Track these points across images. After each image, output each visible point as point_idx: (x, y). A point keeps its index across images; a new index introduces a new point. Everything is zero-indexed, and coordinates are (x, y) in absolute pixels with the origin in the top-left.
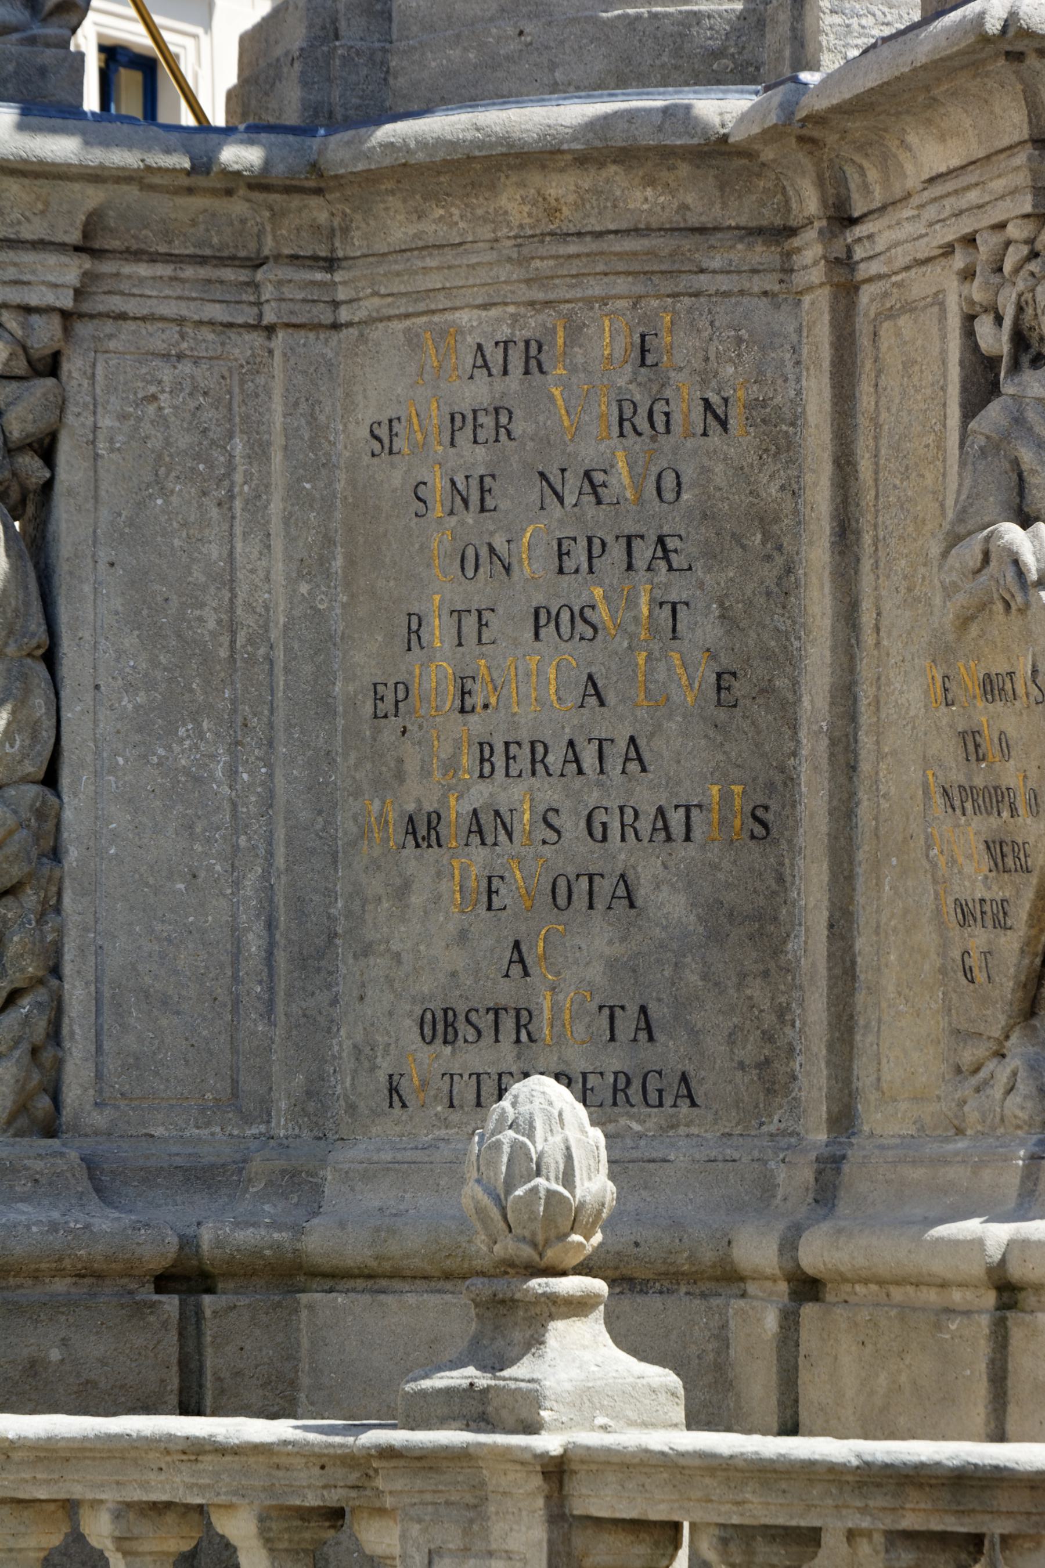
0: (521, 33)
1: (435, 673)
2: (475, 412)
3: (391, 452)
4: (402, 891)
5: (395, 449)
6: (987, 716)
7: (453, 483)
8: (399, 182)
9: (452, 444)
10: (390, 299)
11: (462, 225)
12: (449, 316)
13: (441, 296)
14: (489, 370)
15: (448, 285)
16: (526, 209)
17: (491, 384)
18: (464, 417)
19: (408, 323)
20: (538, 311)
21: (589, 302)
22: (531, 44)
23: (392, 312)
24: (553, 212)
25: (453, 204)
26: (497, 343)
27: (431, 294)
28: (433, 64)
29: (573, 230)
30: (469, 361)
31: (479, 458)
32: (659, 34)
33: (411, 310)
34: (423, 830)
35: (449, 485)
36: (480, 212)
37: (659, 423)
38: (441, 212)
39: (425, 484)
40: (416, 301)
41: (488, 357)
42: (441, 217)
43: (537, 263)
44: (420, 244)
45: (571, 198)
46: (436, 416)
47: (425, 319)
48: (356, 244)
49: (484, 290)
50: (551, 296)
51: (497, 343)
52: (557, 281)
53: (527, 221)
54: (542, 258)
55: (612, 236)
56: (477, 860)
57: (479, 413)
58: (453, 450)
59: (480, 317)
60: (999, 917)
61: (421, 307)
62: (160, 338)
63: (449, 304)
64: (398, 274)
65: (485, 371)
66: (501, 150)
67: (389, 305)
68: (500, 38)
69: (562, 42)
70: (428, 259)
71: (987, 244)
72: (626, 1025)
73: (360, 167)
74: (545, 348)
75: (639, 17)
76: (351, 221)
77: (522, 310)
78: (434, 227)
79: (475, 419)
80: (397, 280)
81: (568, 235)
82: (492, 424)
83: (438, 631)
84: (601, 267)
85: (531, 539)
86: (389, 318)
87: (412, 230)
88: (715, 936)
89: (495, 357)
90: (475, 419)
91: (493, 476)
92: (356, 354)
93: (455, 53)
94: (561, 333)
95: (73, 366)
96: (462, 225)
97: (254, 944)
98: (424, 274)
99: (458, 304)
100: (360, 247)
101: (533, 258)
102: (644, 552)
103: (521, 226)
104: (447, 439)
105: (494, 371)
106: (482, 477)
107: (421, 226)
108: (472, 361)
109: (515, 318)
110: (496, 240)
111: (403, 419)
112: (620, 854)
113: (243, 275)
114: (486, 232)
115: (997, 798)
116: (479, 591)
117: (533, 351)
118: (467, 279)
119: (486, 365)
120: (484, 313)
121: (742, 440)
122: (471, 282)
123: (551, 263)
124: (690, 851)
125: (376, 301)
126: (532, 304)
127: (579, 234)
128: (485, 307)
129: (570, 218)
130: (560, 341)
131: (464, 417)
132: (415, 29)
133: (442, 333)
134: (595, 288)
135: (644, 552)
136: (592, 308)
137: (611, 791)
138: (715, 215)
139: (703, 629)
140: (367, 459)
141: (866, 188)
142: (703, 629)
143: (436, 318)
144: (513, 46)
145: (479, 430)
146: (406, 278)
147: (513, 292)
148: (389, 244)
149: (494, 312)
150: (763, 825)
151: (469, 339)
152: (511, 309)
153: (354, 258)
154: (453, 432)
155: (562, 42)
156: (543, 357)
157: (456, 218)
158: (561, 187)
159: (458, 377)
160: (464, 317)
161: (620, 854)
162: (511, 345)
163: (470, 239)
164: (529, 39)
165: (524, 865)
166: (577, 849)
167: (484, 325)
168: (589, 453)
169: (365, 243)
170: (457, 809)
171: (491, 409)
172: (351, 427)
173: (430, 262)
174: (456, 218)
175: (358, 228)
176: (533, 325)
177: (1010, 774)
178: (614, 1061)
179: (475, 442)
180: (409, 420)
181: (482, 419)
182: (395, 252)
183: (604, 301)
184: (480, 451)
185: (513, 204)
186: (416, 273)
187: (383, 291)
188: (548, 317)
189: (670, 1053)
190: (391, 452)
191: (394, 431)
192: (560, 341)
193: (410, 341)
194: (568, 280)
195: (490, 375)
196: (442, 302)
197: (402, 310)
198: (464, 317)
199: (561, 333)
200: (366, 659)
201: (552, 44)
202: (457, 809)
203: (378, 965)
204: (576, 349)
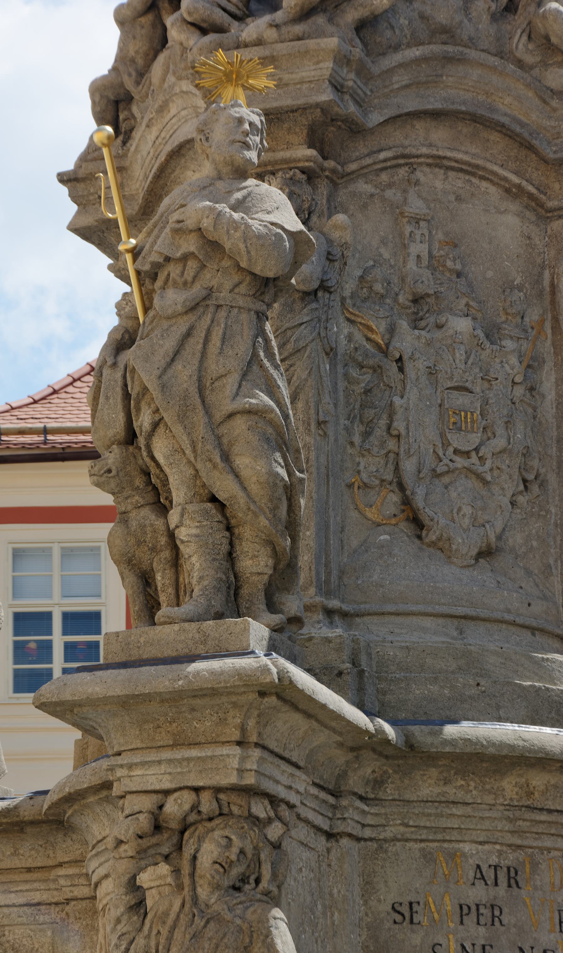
0: (478, 685)
2: (477, 906)
3: (412, 922)
5: (415, 921)
7: (463, 947)
8: (452, 761)
9: (462, 923)
10: (413, 829)
11: (474, 792)
12: (456, 845)
13: (455, 833)
14: (485, 881)
15: (463, 827)
16: (516, 789)
17: (487, 890)
18: (469, 908)
19: (423, 845)
20: (514, 851)
21: (541, 849)
22: (484, 692)
23: (414, 837)
24: (530, 794)
25: (472, 779)
26: (490, 866)
27: (447, 831)
28: (418, 692)
29: (539, 806)
30: (471, 874)
31: (481, 934)
32: (550, 700)
33: (431, 838)
35: (459, 948)
36: (488, 787)
38: (463, 782)
39: (441, 945)
40: (435, 833)
41: (484, 873)
42: (462, 786)
43: (520, 823)
44: (443, 799)
45: (542, 788)
46: (449, 905)
47: (436, 844)
48: (389, 791)
49: (484, 833)
50: (525, 843)
51: (490, 866)
52: (528, 835)
53: (515, 797)
54: (524, 820)
55: (556, 813)
57: (481, 907)
58: (461, 927)
59: (477, 849)
61: (439, 837)
63: (460, 838)
64: (429, 815)
65: (482, 881)
66: (540, 755)
67: (412, 832)
68: (465, 684)
69: (503, 694)
70: (454, 810)
73: (447, 749)
74: (519, 873)
75: (540, 688)
76: (389, 777)
77: (504, 848)
78: (454, 790)
79: (478, 910)
80: (425, 819)
81: (536, 809)
82: (490, 914)
84: (553, 831)
86: (407, 840)
87: (437, 790)
89: (490, 875)
90: (478, 910)
91: (491, 946)
92: (377, 859)
93: (434, 688)
94: (528, 866)
96: (474, 792)
98: (448, 818)
99: (466, 839)
100: (391, 794)
101: (520, 819)
103: (511, 799)
104: (458, 920)
105: (489, 882)
106: (484, 947)
107: (446, 789)
108: (473, 875)
109: (500, 853)
110: (494, 805)
111: (421, 903)
113: (331, 800)
114: (489, 799)
117: (512, 874)
118: (476, 825)
119: (483, 878)
120: (480, 847)
122: (479, 827)
123: (528, 824)
125: (402, 829)
126: (510, 846)
127: (541, 810)
128: (481, 843)
129: (537, 800)
130: (528, 870)
131: (469, 908)
132: (393, 668)
133: (452, 856)
136: (543, 854)
140: (388, 924)
143: (446, 845)
144: (474, 691)
145: (481, 917)
146: (432, 818)
147: (503, 837)
148: (418, 796)
149: (486, 847)
151: (471, 861)
152: (498, 847)
153: (382, 800)
154: (462, 916)
155: (503, 694)
156: (518, 878)
157: (471, 788)
158: (539, 780)
159: (464, 883)
160: (467, 847)
162: (498, 868)
163: (479, 801)
164: (483, 689)
167: (480, 854)
169: (397, 792)
171: (488, 905)
172: (373, 903)
173: (454, 811)
174: (471, 788)
175: (392, 783)
176: (511, 858)
179: (478, 923)
180: (426, 904)
181: (482, 910)
182: (420, 801)
183: (549, 850)
184: (482, 930)
185: (509, 786)
186: (442, 816)
187: (411, 823)
188: (520, 855)
190: (412, 922)
191: (414, 910)
192: (528, 870)
193: (425, 857)
194: (534, 835)
195: (486, 884)
196: (455, 836)
197: (423, 837)
198: (467, 847)
199: (528, 866)
201: (497, 694)
204: (537, 877)
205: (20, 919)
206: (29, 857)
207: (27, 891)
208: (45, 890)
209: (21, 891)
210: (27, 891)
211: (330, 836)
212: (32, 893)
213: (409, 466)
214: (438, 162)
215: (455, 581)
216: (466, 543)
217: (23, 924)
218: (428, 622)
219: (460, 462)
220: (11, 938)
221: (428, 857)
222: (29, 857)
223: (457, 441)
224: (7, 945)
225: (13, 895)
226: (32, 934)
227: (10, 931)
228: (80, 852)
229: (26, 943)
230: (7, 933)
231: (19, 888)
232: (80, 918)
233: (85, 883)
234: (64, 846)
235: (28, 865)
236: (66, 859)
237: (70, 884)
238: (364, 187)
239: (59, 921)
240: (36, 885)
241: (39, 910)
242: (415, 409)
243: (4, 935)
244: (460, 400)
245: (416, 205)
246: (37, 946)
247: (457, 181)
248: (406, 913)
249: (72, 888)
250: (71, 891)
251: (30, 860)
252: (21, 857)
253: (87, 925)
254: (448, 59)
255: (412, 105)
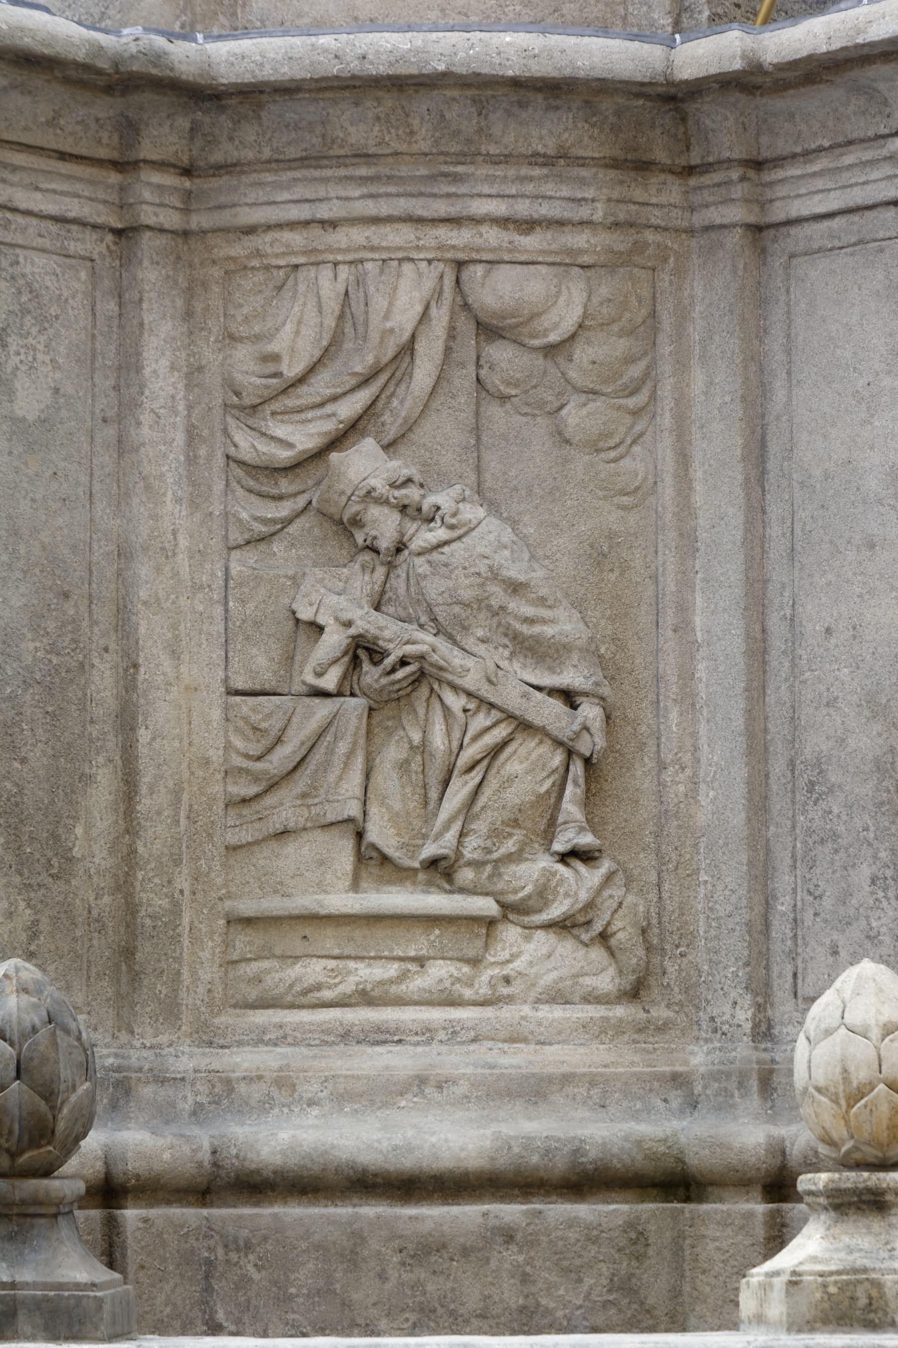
205: (40, 240)
206: (71, 134)
207: (62, 193)
208: (91, 199)
209: (54, 192)
210: (62, 193)
212: (68, 200)
217: (43, 250)
220: (27, 270)
222: (71, 134)
224: (21, 282)
225: (39, 196)
226: (58, 270)
227: (25, 258)
228: (174, 148)
229: (49, 284)
230: (21, 260)
231: (53, 186)
232: (158, 263)
233: (179, 205)
234: (156, 133)
235: (61, 148)
236: (154, 157)
237: (157, 201)
239: (96, 257)
240: (79, 187)
241: (69, 231)
243: (18, 263)
246: (66, 293)
249: (157, 210)
250: (156, 214)
251: (70, 140)
252: (59, 131)
253: (168, 277)
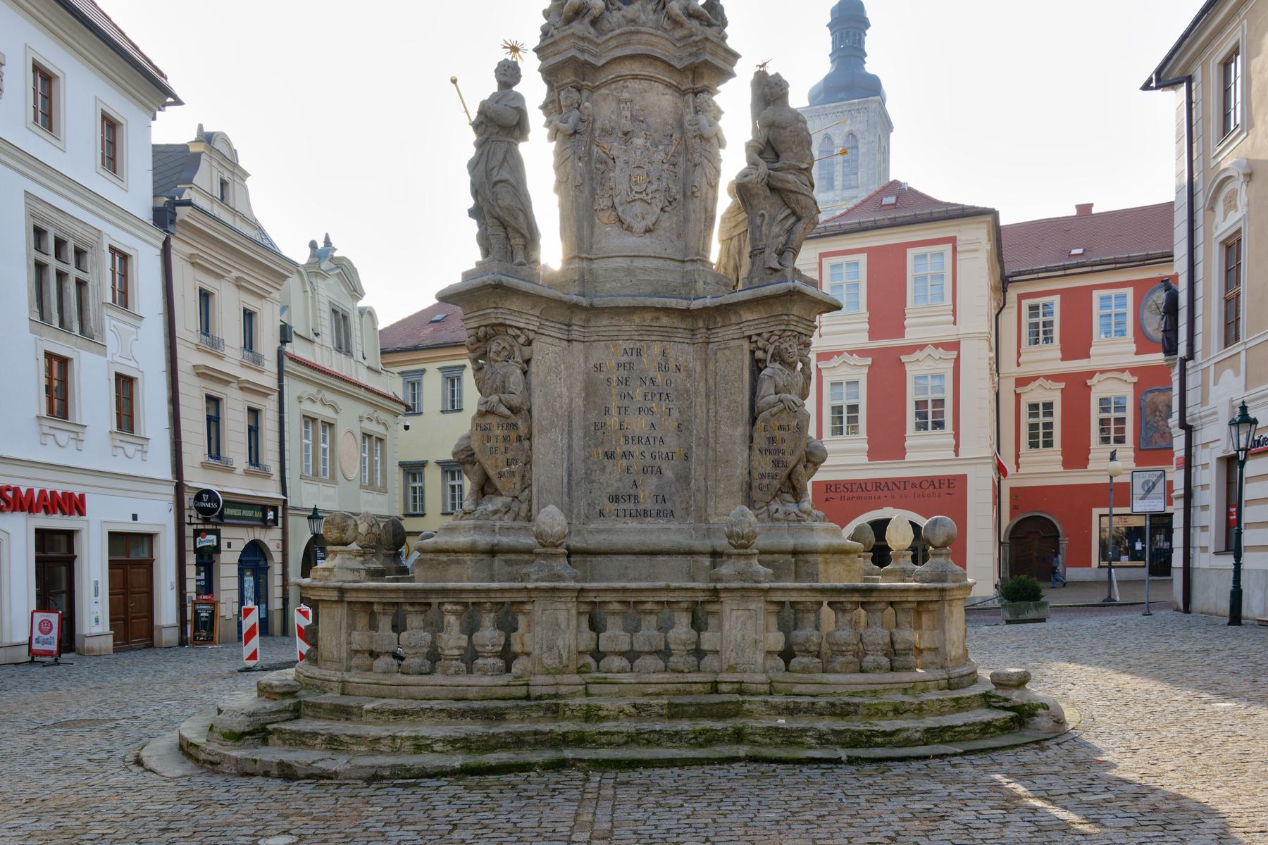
1: (613, 420)
4: (603, 469)
6: (777, 433)
34: (610, 455)
37: (667, 369)
46: (614, 363)
48: (592, 323)
56: (625, 462)
60: (775, 476)
62: (549, 340)
71: (766, 336)
72: (660, 499)
83: (614, 411)
85: (639, 392)
88: (678, 480)
95: (534, 344)
97: (565, 480)
102: (664, 397)
112: (658, 462)
115: (778, 451)
116: (626, 402)
121: (683, 375)
124: (672, 462)
134: (654, 338)
135: (664, 397)
137: (657, 448)
138: (680, 325)
139: (675, 414)
141: (715, 323)
142: (675, 414)
150: (687, 457)
161: (658, 462)
165: (636, 465)
166: (648, 461)
168: (652, 374)
170: (619, 451)
176: (638, 345)
177: (784, 446)
178: (657, 507)
185: (637, 319)
189: (669, 506)
200: (593, 416)
202: (619, 451)
203: (596, 485)
211: (569, 341)
213: (617, 200)
214: (635, 77)
215: (630, 242)
216: (639, 226)
218: (620, 260)
219: (637, 196)
221: (607, 347)
223: (636, 188)
238: (604, 91)
242: (618, 176)
244: (638, 171)
245: (626, 95)
247: (645, 84)
248: (598, 368)
254: (632, 33)
255: (618, 53)
